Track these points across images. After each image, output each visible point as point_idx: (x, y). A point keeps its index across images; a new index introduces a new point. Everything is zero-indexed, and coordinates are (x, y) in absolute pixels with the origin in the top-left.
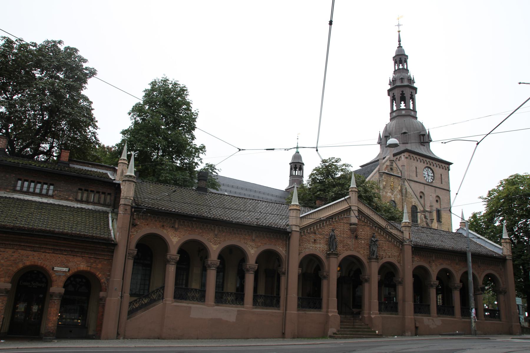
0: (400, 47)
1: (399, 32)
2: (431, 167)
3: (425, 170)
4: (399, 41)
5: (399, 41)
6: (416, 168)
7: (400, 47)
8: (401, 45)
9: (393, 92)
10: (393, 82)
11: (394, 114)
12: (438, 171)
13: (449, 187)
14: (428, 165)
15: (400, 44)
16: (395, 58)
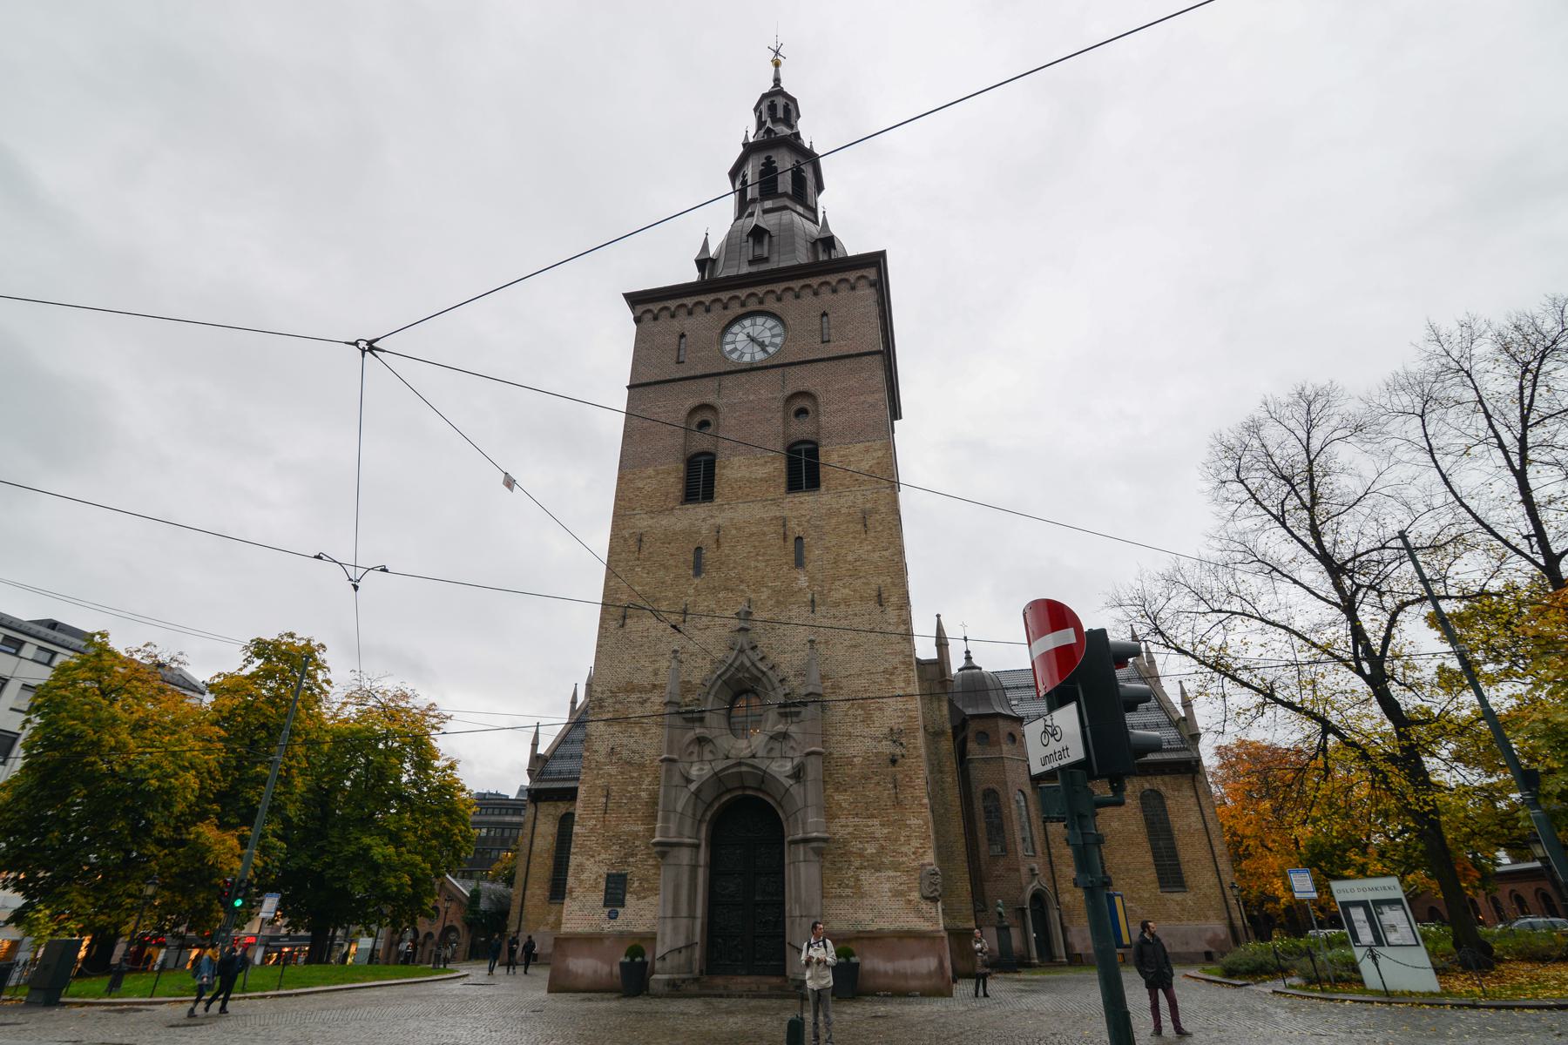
1: (777, 64)
2: (771, 304)
3: (736, 328)
14: (753, 305)
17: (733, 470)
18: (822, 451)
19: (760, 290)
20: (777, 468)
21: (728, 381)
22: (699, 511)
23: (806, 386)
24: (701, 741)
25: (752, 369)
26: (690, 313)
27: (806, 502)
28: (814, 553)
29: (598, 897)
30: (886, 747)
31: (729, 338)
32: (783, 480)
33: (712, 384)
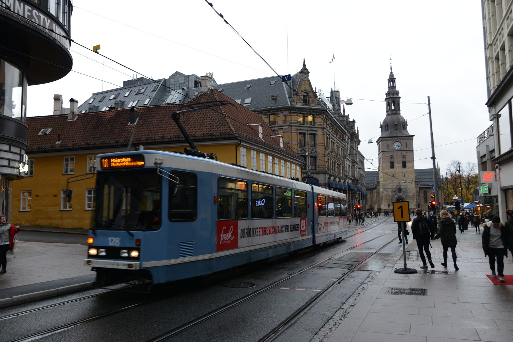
0: (391, 73)
1: (391, 63)
2: (399, 141)
3: (395, 143)
4: (391, 69)
5: (391, 69)
6: (388, 144)
7: (391, 73)
8: (392, 72)
9: (389, 100)
10: (388, 94)
11: (389, 112)
12: (404, 142)
13: (413, 149)
14: (397, 141)
15: (391, 71)
16: (389, 80)
17: (396, 165)
18: (406, 163)
19: (398, 138)
20: (401, 165)
21: (395, 152)
22: (392, 170)
23: (404, 154)
24: (396, 194)
25: (397, 151)
26: (389, 140)
27: (405, 170)
28: (405, 176)
29: (387, 206)
30: (413, 195)
31: (394, 145)
32: (402, 166)
33: (393, 152)
